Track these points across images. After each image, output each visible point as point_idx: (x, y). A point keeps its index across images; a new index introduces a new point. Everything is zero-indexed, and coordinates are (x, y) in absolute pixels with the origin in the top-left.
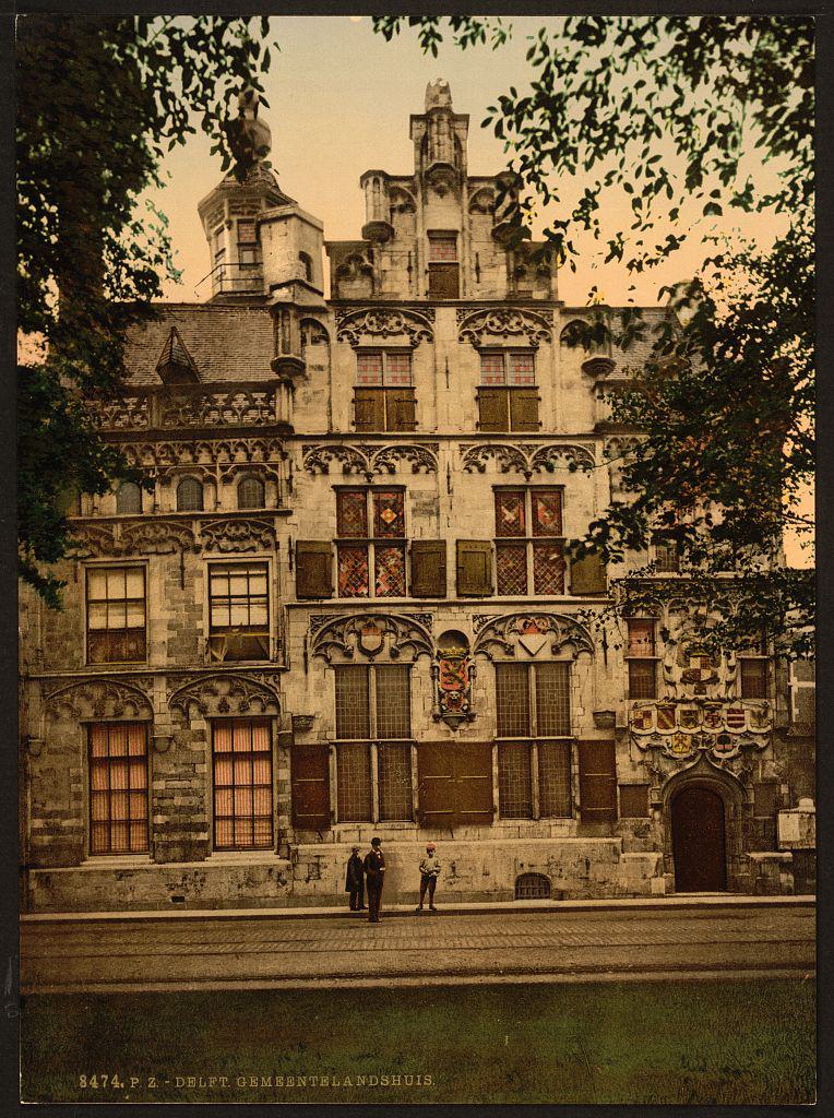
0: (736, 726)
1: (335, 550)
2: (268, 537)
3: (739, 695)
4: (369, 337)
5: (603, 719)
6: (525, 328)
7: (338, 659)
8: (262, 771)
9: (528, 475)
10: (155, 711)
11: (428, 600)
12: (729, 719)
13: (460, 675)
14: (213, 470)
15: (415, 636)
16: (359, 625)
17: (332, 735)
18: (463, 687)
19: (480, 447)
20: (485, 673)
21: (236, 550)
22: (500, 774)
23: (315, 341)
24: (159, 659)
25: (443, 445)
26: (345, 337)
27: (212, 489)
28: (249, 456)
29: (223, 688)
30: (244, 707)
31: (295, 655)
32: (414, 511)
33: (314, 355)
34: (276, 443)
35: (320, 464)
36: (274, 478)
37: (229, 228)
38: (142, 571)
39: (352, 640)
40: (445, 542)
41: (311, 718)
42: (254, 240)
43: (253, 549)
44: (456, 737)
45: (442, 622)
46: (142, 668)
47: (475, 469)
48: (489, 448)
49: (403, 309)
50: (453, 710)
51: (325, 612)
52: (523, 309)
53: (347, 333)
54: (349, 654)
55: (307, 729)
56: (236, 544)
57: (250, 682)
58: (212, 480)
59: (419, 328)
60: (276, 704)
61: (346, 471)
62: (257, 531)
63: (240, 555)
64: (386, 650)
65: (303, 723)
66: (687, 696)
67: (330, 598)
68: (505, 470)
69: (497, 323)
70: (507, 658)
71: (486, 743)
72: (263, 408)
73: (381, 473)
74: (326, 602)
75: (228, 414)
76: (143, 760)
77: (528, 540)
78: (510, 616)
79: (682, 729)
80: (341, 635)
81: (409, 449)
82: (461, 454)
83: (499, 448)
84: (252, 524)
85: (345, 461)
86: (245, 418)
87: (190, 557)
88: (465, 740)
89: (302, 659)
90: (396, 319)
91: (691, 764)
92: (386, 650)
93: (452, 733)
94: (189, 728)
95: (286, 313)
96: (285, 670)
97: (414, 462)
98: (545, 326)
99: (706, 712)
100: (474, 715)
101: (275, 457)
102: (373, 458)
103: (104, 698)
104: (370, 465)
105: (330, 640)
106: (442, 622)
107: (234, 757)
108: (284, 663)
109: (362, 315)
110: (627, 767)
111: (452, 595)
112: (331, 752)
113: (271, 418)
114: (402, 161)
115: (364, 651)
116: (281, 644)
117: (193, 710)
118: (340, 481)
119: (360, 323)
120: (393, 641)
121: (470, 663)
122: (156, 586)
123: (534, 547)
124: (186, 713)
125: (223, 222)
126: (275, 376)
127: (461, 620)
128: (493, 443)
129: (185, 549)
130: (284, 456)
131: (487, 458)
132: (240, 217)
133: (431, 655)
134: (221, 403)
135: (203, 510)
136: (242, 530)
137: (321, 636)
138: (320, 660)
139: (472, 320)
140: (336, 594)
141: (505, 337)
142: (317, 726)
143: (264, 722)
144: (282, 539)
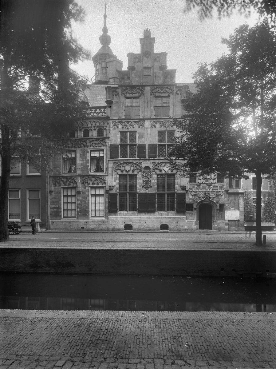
0: (215, 190)
1: (120, 146)
2: (104, 144)
3: (217, 182)
4: (129, 94)
5: (183, 188)
6: (167, 91)
7: (120, 172)
8: (102, 199)
9: (166, 128)
10: (78, 184)
11: (141, 159)
12: (214, 188)
13: (148, 177)
14: (92, 127)
15: (138, 167)
16: (125, 165)
17: (118, 191)
18: (149, 180)
19: (155, 121)
20: (155, 176)
21: (96, 147)
22: (158, 200)
23: (116, 96)
24: (79, 172)
25: (146, 121)
26: (123, 94)
27: (91, 132)
28: (100, 124)
29: (93, 179)
30: (98, 184)
31: (110, 172)
32: (139, 137)
33: (115, 100)
34: (106, 121)
35: (116, 126)
36: (105, 129)
37: (100, 64)
38: (75, 151)
39: (123, 168)
40: (145, 145)
41: (113, 187)
42: (105, 66)
43: (100, 146)
44: (147, 191)
45: (144, 164)
46: (75, 174)
47: (153, 127)
48: (157, 121)
49: (137, 87)
50: (147, 186)
51: (117, 162)
52: (166, 87)
53: (123, 93)
54: (122, 172)
55: (112, 189)
56: (97, 145)
57: (99, 178)
58: (91, 130)
59: (141, 92)
60: (105, 183)
61: (123, 127)
62: (102, 142)
63: (97, 148)
64: (131, 171)
65: (111, 188)
66: (204, 182)
67: (118, 158)
68: (161, 127)
69: (160, 90)
70: (160, 173)
71: (155, 193)
72: (103, 112)
73: (131, 128)
74: (117, 159)
75: (95, 114)
76: (75, 196)
77: (166, 144)
78: (161, 163)
79: (202, 190)
80: (120, 167)
81: (138, 122)
82: (150, 123)
83: (160, 121)
84: (101, 140)
85: (122, 125)
86: (99, 115)
87: (86, 148)
88: (149, 192)
89: (111, 173)
90: (135, 90)
91: (204, 199)
92: (131, 171)
93: (146, 191)
94: (85, 188)
95: (109, 89)
96: (107, 175)
97: (139, 125)
98: (172, 90)
99: (208, 186)
100: (151, 186)
101: (106, 124)
102: (129, 124)
103: (66, 181)
104: (128, 125)
105: (118, 168)
106: (144, 164)
107: (95, 195)
108: (107, 174)
109: (127, 89)
110: (189, 199)
111: (147, 158)
112: (118, 195)
113: (105, 115)
114: (137, 50)
115: (126, 171)
116: (107, 169)
117: (86, 184)
118: (121, 130)
119: (127, 91)
120: (133, 168)
121: (151, 174)
122: (78, 155)
123: (168, 146)
124: (85, 185)
125: (98, 62)
126: (106, 105)
127: (149, 164)
128: (158, 120)
129: (85, 146)
130: (108, 124)
131: (156, 124)
132: (102, 61)
133: (142, 172)
134: (94, 111)
135: (89, 137)
136: (98, 142)
137: (116, 168)
138: (116, 173)
139: (154, 90)
140: (120, 157)
141: (162, 94)
142: (115, 188)
143: (103, 187)
144: (107, 144)
